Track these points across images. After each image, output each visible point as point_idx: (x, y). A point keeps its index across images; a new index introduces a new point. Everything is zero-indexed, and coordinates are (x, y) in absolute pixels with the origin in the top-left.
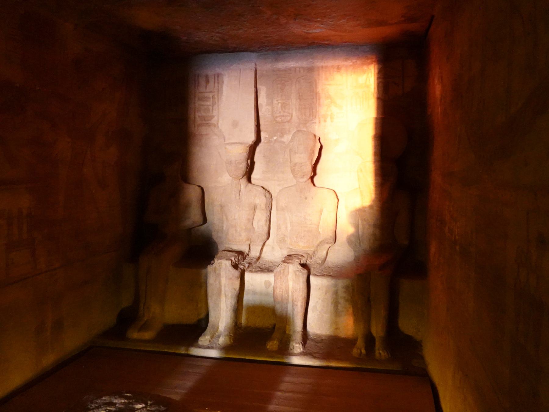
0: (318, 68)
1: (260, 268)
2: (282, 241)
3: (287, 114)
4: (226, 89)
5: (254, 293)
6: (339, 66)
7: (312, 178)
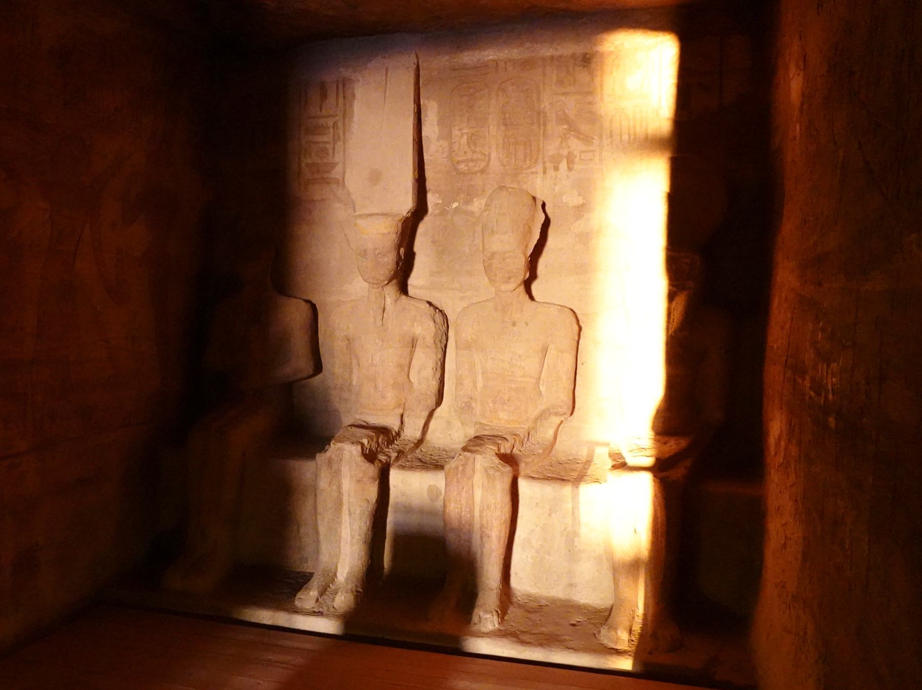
0: (544, 59)
1: (420, 460)
2: (466, 408)
3: (480, 156)
4: (358, 109)
5: (408, 509)
6: (585, 54)
7: (527, 285)
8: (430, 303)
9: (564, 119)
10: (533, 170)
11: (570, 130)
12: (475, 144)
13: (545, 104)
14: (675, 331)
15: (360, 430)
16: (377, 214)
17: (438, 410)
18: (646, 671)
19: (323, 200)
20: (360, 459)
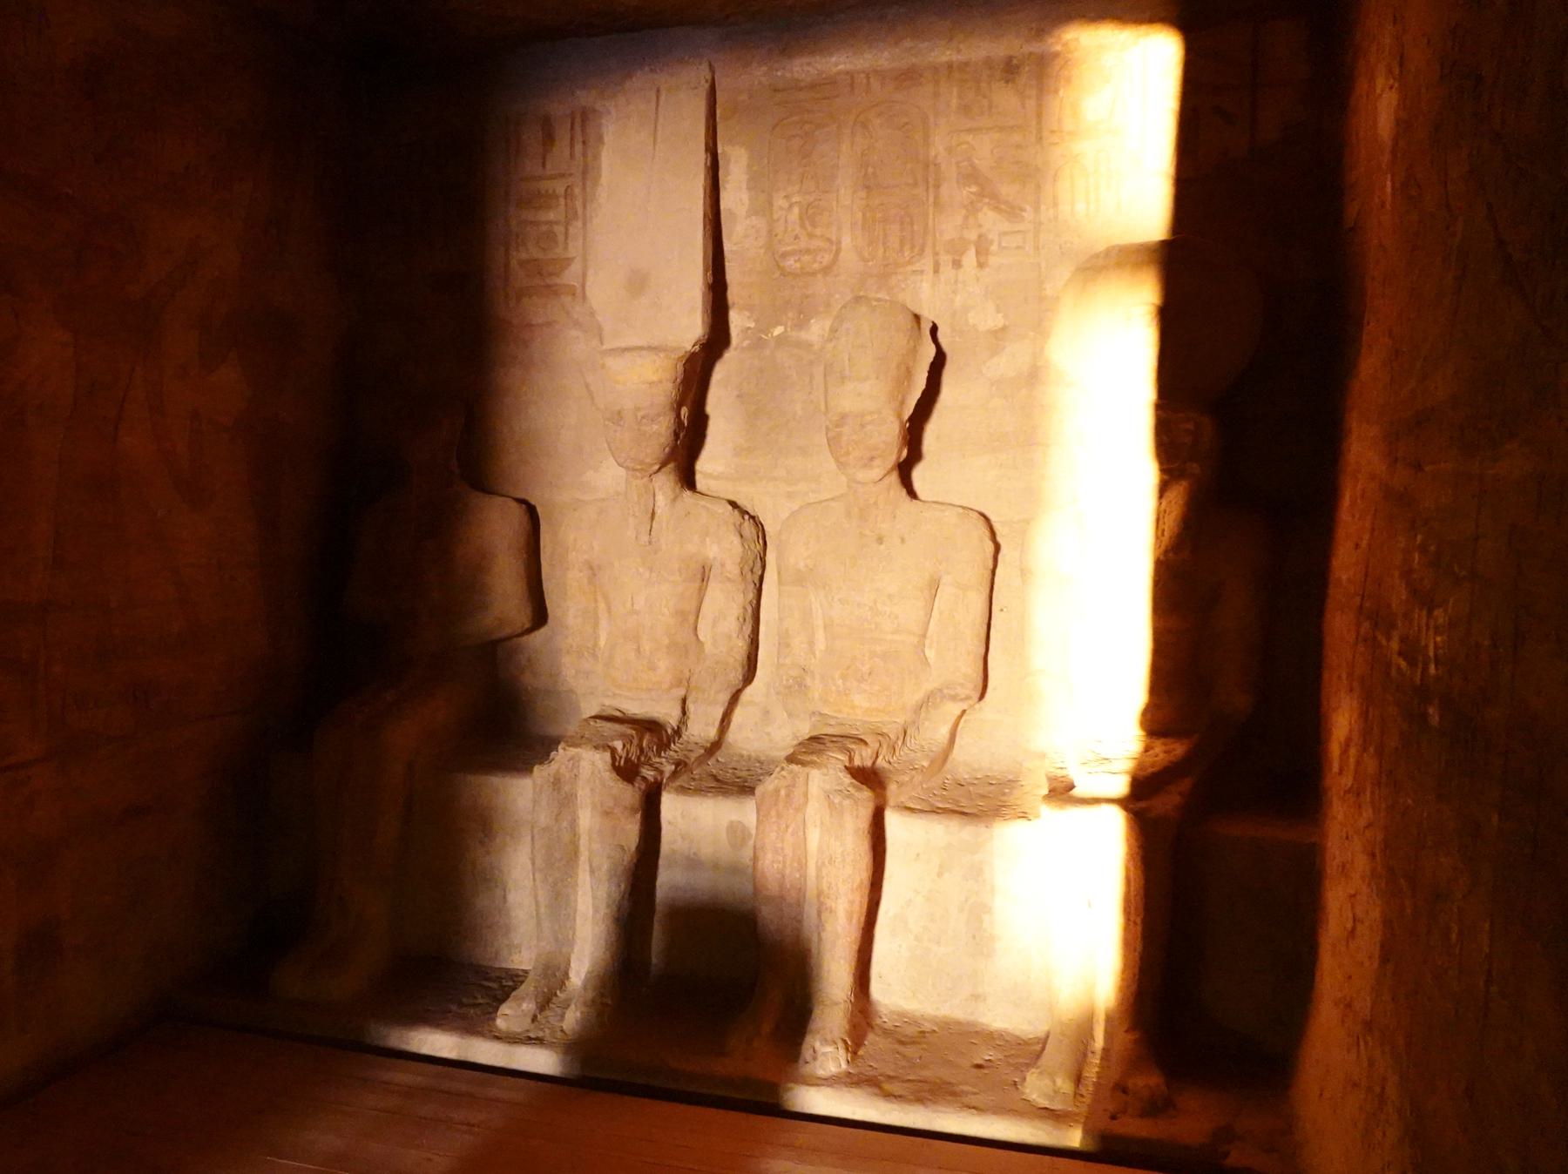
0: (935, 69)
1: (715, 778)
4: (608, 161)
5: (693, 863)
6: (1011, 58)
8: (733, 504)
9: (972, 176)
10: (917, 267)
11: (981, 195)
12: (814, 225)
13: (938, 147)
14: (1166, 552)
15: (609, 725)
16: (641, 348)
17: (749, 690)
18: (1105, 1149)
19: (549, 324)
20: (609, 777)
